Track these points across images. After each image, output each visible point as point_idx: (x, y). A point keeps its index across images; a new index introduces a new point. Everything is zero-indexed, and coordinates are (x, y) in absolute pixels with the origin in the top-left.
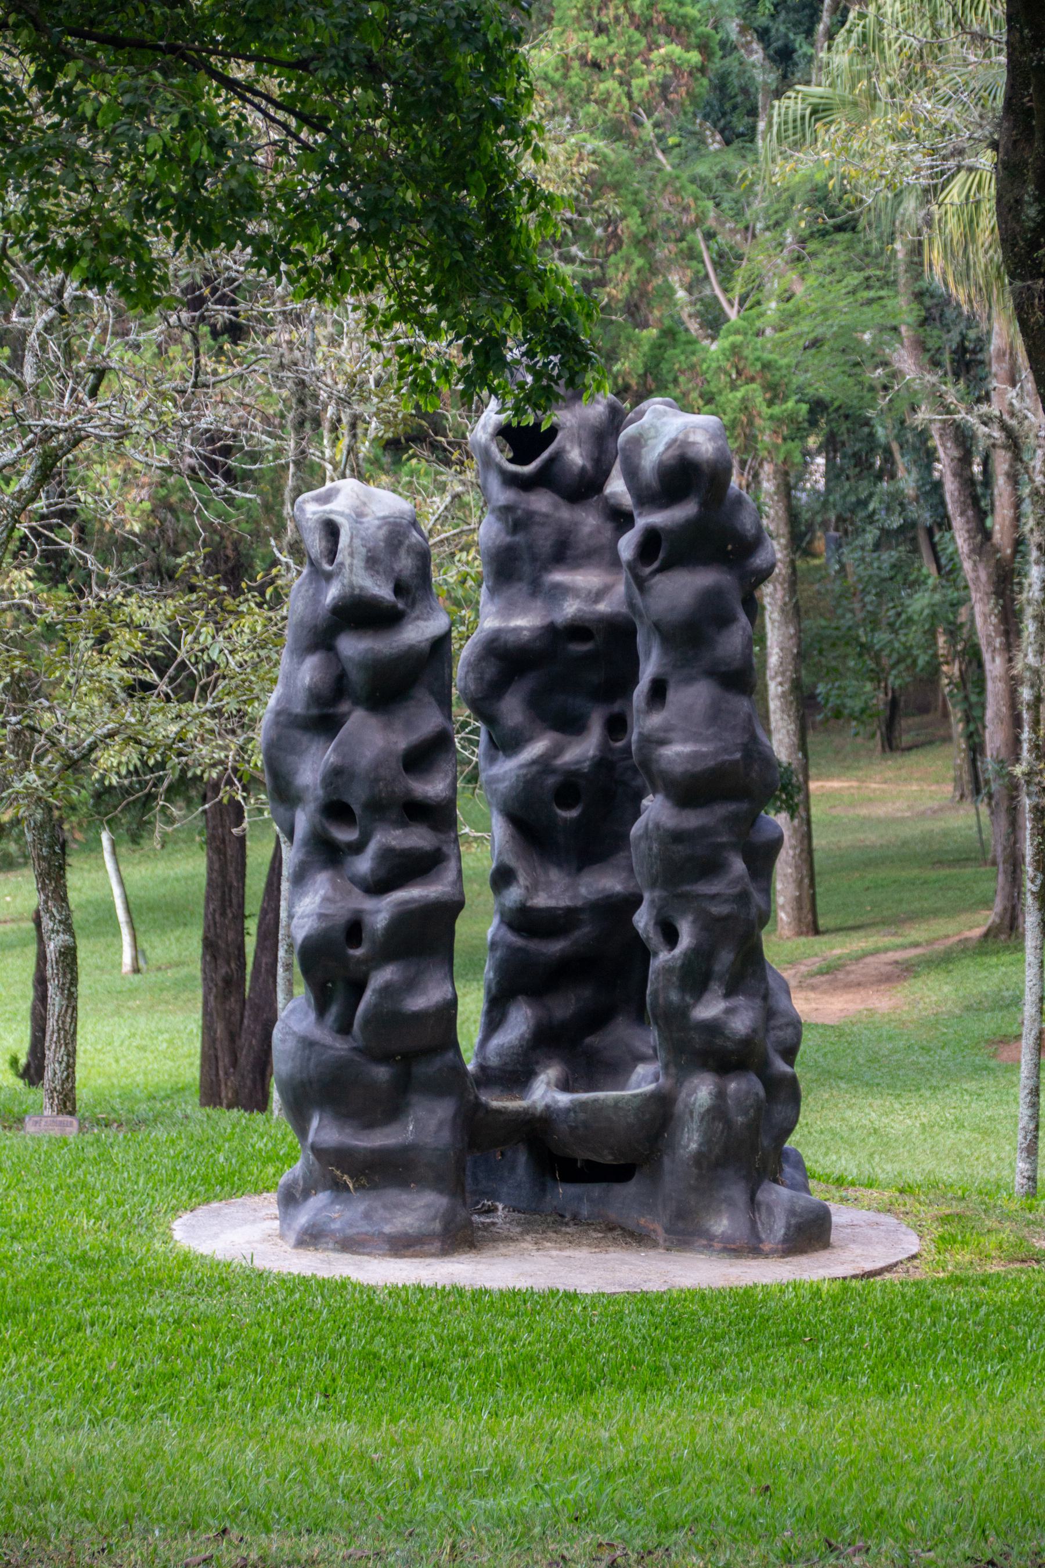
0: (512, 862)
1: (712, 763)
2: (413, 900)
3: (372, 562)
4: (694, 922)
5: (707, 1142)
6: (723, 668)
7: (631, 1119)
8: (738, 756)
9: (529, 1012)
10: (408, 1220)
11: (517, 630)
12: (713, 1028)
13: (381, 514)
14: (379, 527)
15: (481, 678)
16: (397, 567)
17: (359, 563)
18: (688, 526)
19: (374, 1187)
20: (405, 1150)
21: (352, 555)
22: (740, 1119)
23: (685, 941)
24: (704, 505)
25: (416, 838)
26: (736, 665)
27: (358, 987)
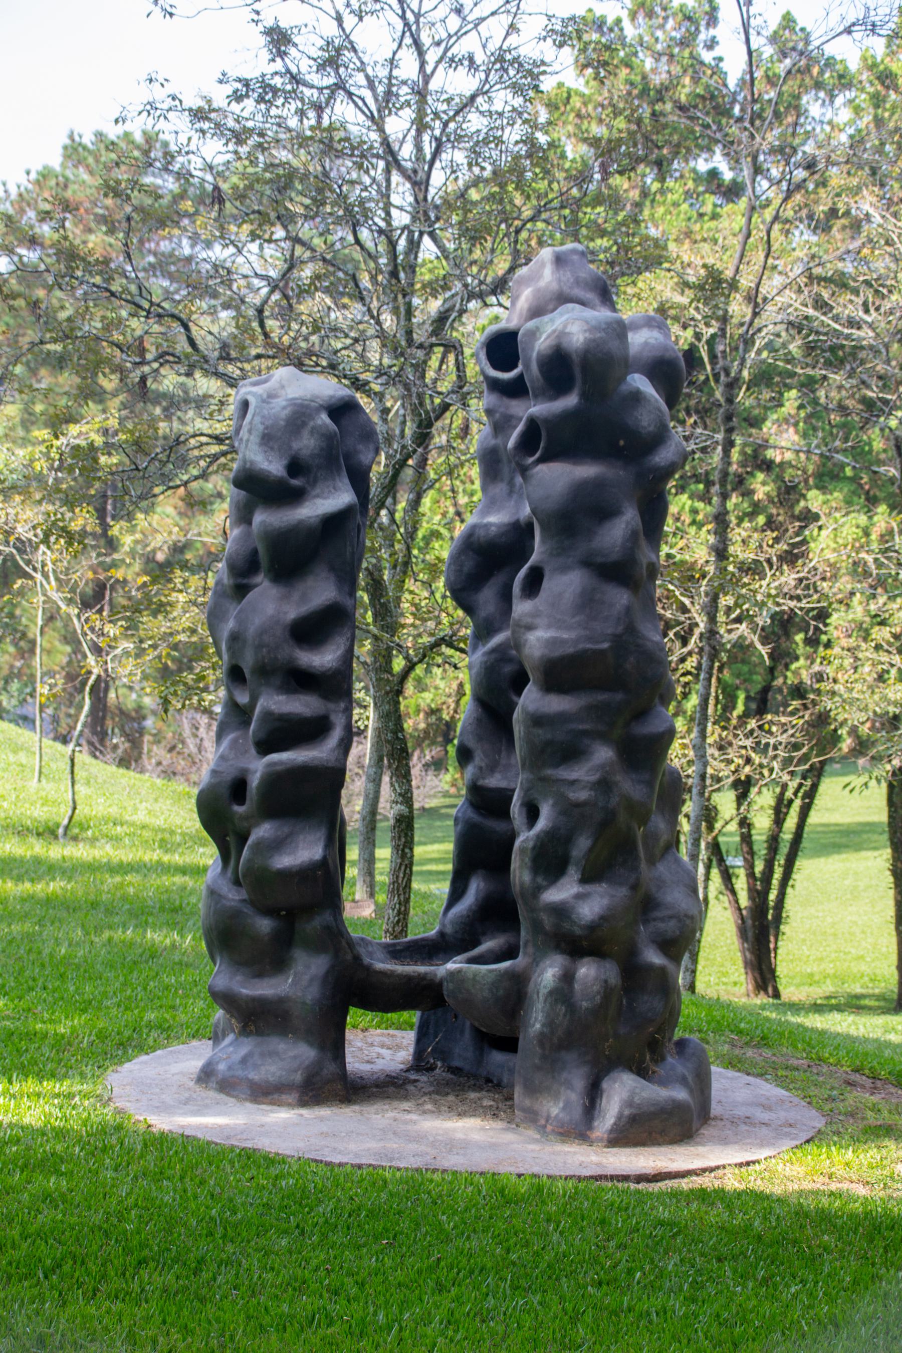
0: (471, 743)
1: (571, 650)
2: (280, 763)
3: (267, 439)
4: (553, 806)
5: (550, 1023)
6: (600, 560)
7: (486, 994)
8: (606, 645)
9: (482, 885)
10: (273, 1069)
11: (487, 526)
12: (561, 911)
13: (290, 396)
14: (284, 408)
15: (461, 571)
16: (295, 445)
17: (255, 439)
18: (566, 416)
19: (259, 1033)
20: (281, 1001)
21: (250, 431)
22: (584, 1004)
23: (542, 824)
24: (584, 396)
25: (301, 705)
26: (614, 557)
27: (243, 838)
